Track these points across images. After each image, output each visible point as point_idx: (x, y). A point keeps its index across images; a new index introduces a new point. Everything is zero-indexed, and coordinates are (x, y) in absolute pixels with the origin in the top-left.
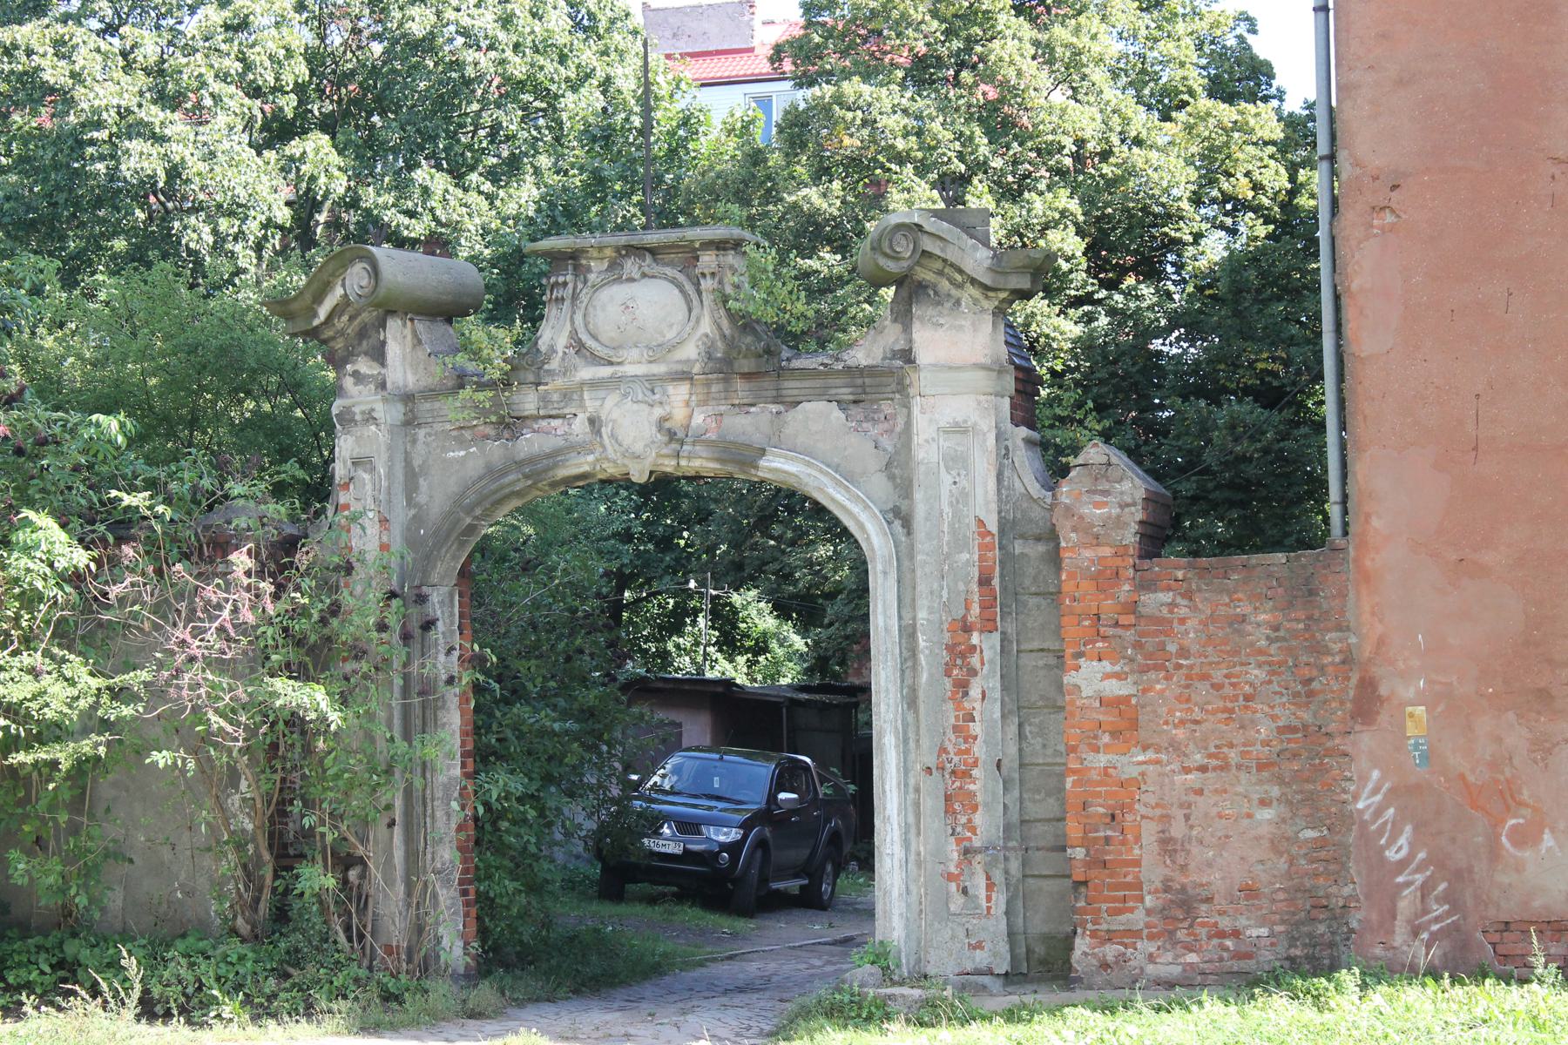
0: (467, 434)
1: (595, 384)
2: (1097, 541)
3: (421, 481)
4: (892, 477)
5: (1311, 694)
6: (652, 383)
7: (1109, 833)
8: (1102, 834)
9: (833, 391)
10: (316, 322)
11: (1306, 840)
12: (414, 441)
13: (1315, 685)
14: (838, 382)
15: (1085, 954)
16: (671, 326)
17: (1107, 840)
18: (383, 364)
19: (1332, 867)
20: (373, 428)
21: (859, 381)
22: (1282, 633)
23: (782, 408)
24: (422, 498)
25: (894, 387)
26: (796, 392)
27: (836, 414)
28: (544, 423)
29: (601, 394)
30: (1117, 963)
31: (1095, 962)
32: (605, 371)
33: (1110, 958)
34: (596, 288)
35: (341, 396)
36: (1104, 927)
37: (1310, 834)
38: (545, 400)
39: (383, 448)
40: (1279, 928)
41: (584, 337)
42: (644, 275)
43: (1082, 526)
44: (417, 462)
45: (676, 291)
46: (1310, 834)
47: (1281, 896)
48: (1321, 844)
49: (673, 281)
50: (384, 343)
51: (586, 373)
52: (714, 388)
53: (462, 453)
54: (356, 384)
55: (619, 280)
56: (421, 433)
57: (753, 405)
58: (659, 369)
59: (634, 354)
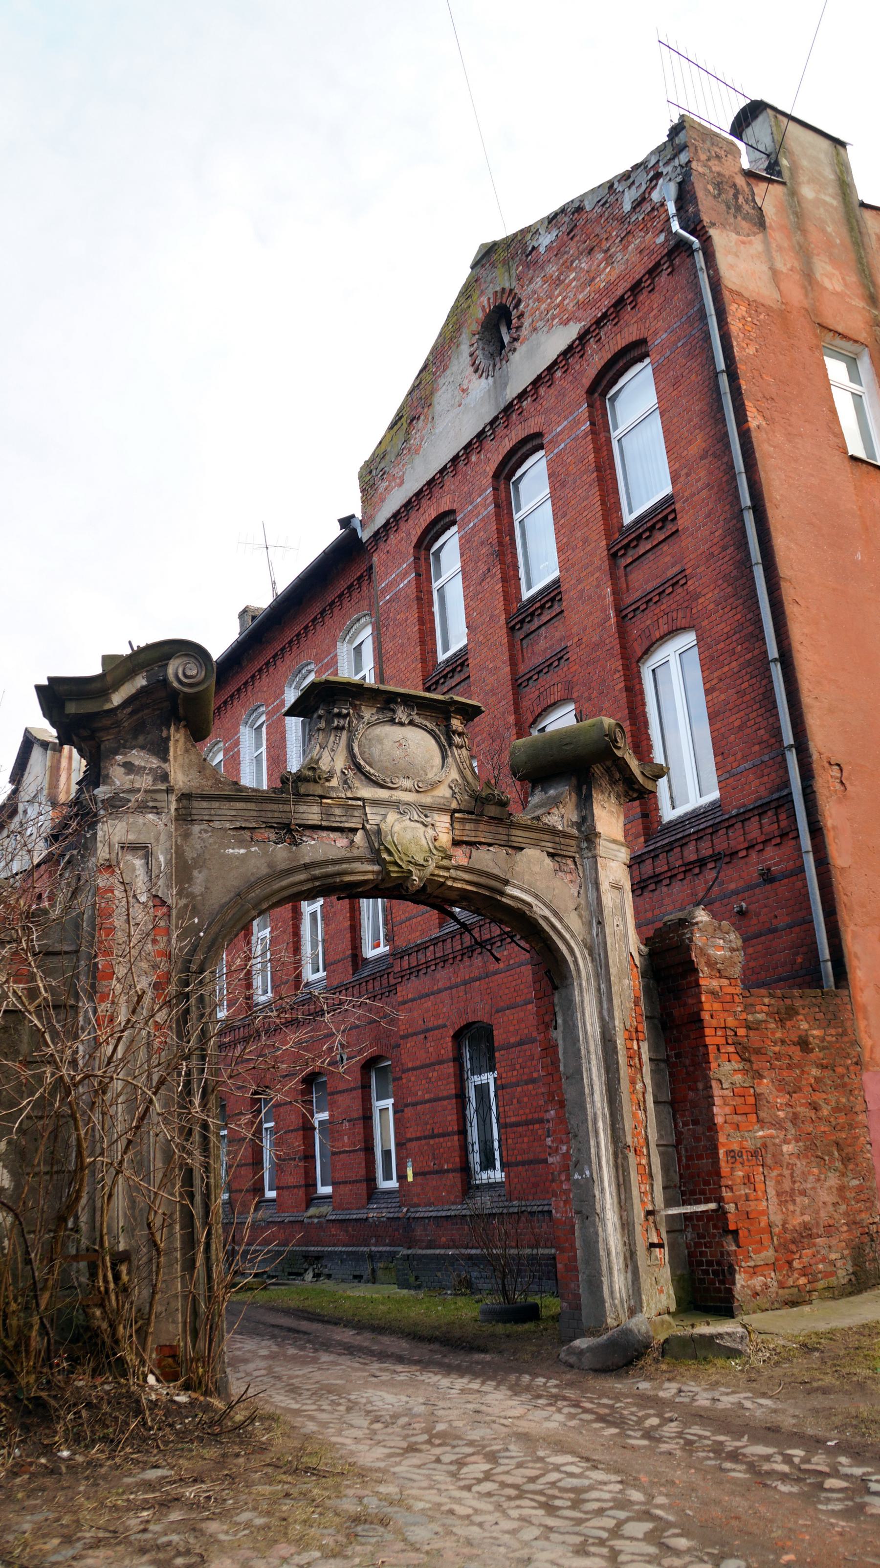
0: (247, 835)
1: (376, 803)
2: (721, 975)
3: (195, 873)
4: (580, 916)
5: (844, 1085)
6: (426, 809)
7: (747, 1191)
8: (743, 1192)
9: (543, 844)
10: (108, 706)
11: (854, 1187)
12: (187, 835)
13: (846, 1079)
14: (546, 837)
15: (743, 1286)
16: (432, 767)
17: (747, 1198)
18: (165, 760)
19: (868, 1204)
20: (151, 816)
21: (557, 839)
22: (825, 1044)
23: (510, 851)
24: (197, 888)
25: (574, 849)
26: (520, 840)
27: (548, 861)
28: (324, 834)
29: (382, 811)
30: (762, 1290)
31: (749, 1292)
32: (383, 794)
33: (758, 1288)
34: (370, 725)
35: (105, 784)
36: (752, 1264)
37: (855, 1182)
38: (327, 813)
39: (163, 838)
40: (846, 1252)
41: (362, 763)
42: (411, 723)
43: (711, 964)
44: (190, 854)
45: (433, 741)
46: (855, 1182)
47: (845, 1228)
48: (859, 1190)
49: (431, 732)
50: (168, 739)
51: (367, 792)
52: (468, 826)
53: (242, 851)
54: (128, 774)
55: (392, 721)
56: (196, 828)
57: (490, 845)
58: (427, 799)
59: (407, 783)
